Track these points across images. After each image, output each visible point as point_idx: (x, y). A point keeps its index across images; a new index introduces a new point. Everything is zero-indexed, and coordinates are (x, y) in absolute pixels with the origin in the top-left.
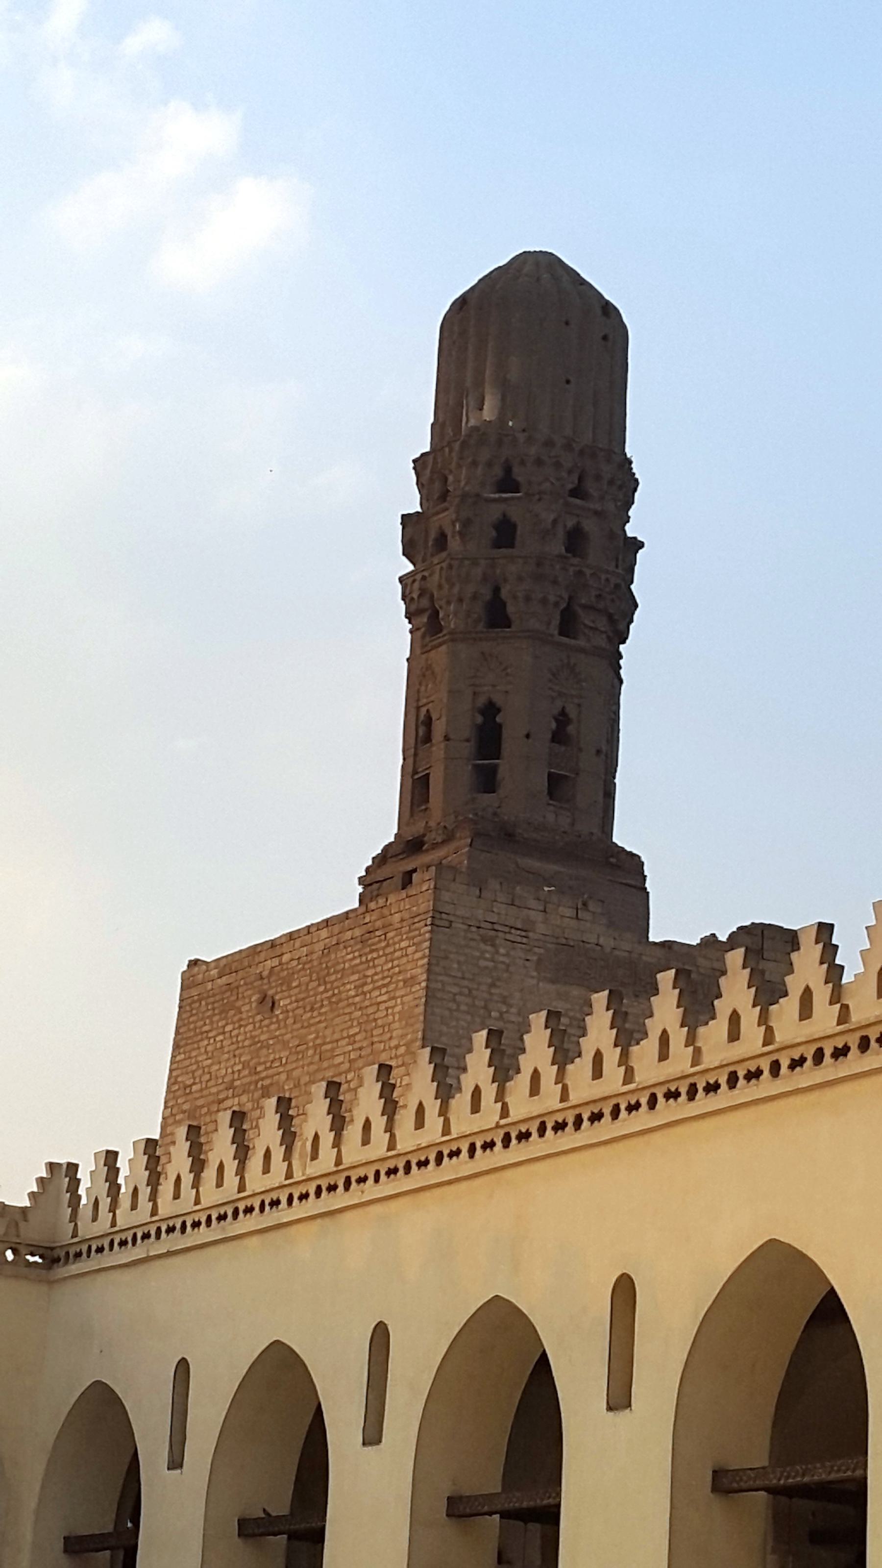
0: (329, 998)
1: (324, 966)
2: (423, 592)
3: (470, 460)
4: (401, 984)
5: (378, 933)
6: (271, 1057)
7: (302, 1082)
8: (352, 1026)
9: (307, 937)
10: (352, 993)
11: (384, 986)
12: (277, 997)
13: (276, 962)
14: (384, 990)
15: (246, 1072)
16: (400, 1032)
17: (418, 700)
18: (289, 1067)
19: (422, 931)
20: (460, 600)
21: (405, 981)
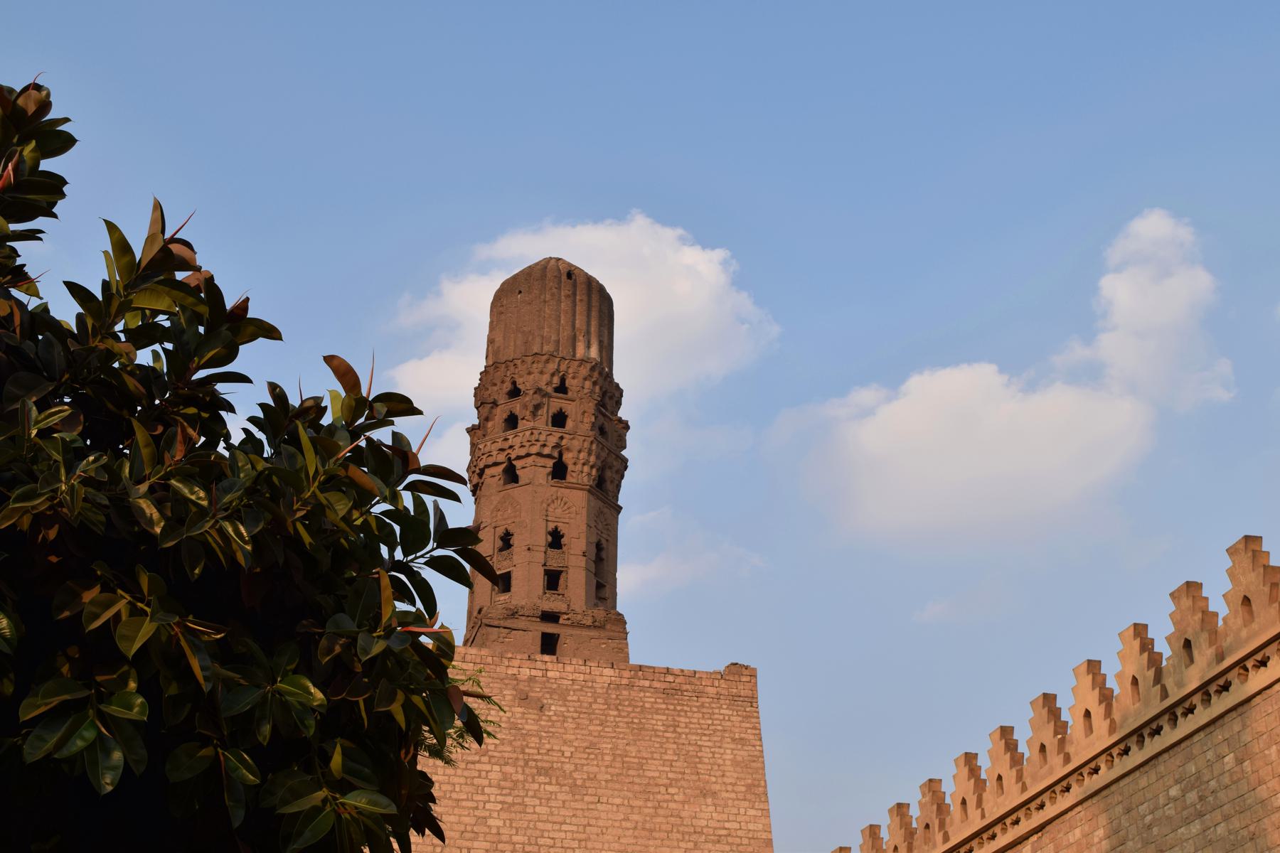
0: (627, 723)
1: (614, 696)
2: (557, 446)
3: (593, 380)
4: (729, 740)
5: (685, 693)
6: (548, 746)
7: (599, 777)
8: (665, 753)
9: (583, 668)
10: (661, 728)
11: (705, 735)
12: (545, 701)
13: (534, 673)
14: (704, 738)
15: (509, 749)
16: (735, 775)
17: (547, 516)
18: (577, 761)
19: (748, 709)
20: (592, 467)
21: (734, 740)
